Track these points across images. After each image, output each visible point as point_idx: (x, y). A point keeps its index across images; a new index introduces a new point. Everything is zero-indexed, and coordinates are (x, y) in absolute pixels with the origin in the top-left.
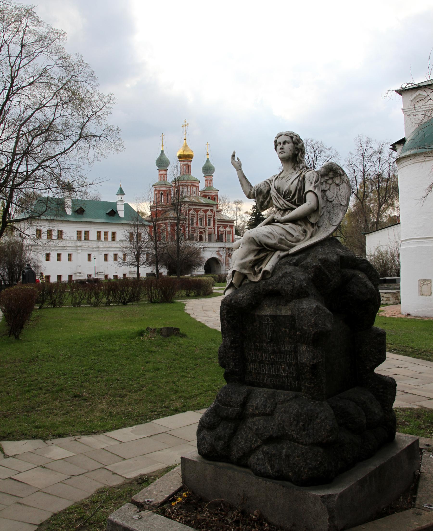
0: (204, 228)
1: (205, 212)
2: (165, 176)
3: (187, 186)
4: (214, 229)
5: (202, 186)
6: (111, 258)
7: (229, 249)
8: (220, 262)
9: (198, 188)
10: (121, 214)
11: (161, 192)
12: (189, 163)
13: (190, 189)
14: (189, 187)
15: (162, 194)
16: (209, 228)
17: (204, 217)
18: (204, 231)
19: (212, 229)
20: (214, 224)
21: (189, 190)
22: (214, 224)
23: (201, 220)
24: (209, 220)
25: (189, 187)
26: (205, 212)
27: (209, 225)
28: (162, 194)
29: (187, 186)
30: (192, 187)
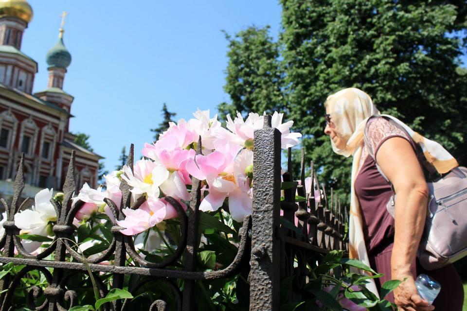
0: (32, 160)
1: (41, 124)
4: (55, 165)
5: (43, 82)
9: (30, 76)
12: (20, 27)
14: (10, 68)
16: (43, 163)
17: (36, 135)
18: (31, 165)
19: (49, 164)
20: (56, 156)
21: (9, 73)
22: (56, 156)
23: (27, 139)
24: (47, 145)
25: (10, 68)
26: (41, 124)
27: (46, 155)
30: (16, 70)
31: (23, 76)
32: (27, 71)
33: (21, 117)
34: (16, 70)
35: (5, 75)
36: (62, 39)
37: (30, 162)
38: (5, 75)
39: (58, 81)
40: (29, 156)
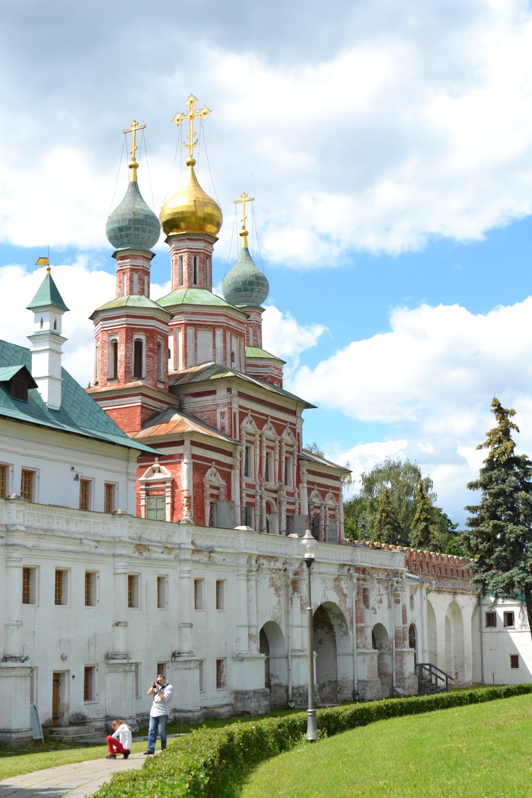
0: (275, 492)
2: (146, 278)
3: (213, 328)
6: (45, 585)
7: (363, 570)
8: (335, 622)
10: (45, 392)
11: (136, 336)
13: (225, 341)
14: (219, 333)
15: (138, 345)
18: (275, 499)
20: (299, 481)
21: (219, 343)
22: (299, 481)
25: (219, 333)
28: (138, 345)
29: (213, 328)
30: (228, 334)
31: (235, 344)
32: (239, 334)
33: (260, 422)
34: (228, 334)
35: (214, 347)
36: (135, 184)
37: (274, 495)
38: (214, 347)
39: (142, 282)
40: (272, 484)
